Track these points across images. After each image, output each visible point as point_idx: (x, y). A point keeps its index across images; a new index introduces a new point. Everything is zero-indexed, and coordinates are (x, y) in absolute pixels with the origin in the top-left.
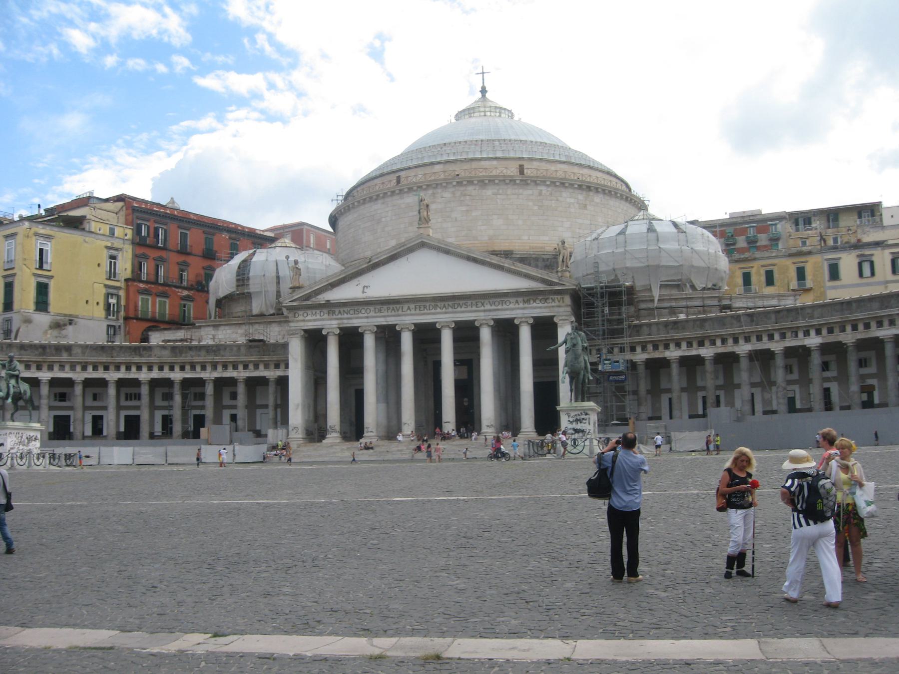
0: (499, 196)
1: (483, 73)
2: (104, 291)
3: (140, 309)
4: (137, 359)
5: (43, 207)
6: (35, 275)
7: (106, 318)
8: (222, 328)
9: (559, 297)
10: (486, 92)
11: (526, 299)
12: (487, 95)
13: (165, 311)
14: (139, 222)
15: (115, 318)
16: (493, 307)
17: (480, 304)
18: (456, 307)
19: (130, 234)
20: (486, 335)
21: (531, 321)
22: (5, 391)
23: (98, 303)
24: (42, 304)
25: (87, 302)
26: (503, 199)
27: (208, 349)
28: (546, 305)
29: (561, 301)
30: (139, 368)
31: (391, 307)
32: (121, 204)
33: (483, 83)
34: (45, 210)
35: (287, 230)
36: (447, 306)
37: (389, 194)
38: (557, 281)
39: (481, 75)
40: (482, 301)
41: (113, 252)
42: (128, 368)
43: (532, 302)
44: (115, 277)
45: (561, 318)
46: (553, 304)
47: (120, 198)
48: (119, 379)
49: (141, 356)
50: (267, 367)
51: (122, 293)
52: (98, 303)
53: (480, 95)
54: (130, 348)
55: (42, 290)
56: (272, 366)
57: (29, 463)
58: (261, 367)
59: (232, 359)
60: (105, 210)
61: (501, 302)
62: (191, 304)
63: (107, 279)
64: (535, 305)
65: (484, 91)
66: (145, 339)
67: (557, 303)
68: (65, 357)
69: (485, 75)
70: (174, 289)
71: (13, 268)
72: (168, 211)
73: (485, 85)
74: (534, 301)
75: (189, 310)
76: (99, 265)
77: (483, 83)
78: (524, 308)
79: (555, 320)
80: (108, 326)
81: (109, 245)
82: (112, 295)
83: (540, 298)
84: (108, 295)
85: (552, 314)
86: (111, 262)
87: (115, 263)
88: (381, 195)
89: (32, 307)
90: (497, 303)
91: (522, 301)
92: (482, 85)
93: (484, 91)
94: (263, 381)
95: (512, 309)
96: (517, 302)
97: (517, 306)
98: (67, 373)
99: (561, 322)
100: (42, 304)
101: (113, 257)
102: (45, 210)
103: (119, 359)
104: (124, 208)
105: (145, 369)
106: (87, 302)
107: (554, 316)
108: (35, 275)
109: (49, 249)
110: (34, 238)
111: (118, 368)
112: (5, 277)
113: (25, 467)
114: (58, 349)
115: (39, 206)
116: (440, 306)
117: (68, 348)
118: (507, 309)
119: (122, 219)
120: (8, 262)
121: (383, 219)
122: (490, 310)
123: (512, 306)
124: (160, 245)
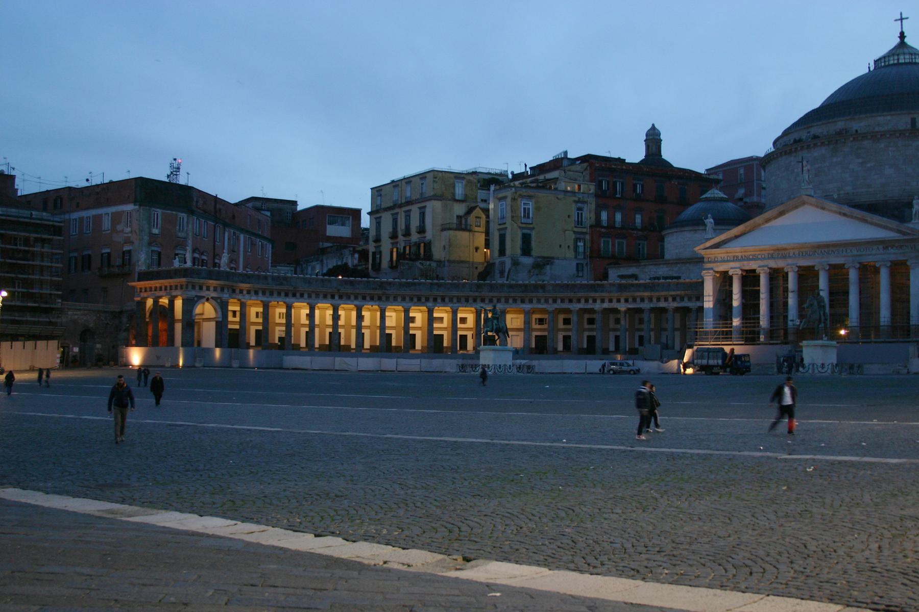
0: (890, 149)
1: (901, 19)
2: (573, 236)
3: (602, 249)
4: (592, 294)
5: (530, 165)
6: (520, 228)
7: (576, 257)
8: (662, 266)
10: (905, 37)
12: (906, 40)
13: (623, 250)
14: (600, 178)
15: (583, 257)
16: (859, 253)
17: (849, 251)
19: (592, 188)
20: (853, 275)
21: (889, 264)
22: (491, 327)
23: (569, 247)
24: (526, 250)
25: (560, 246)
26: (894, 151)
27: (646, 287)
30: (595, 301)
31: (781, 253)
32: (585, 165)
33: (902, 28)
34: (530, 168)
35: (740, 165)
37: (799, 148)
38: (910, 232)
39: (899, 22)
41: (579, 205)
42: (587, 301)
43: (890, 248)
44: (582, 225)
47: (588, 159)
48: (580, 309)
49: (596, 291)
50: (690, 299)
51: (588, 237)
52: (569, 247)
53: (898, 40)
54: (588, 285)
55: (526, 239)
56: (694, 299)
57: (505, 370)
58: (686, 299)
59: (663, 293)
60: (573, 171)
62: (646, 243)
63: (576, 227)
64: (892, 251)
65: (902, 36)
66: (605, 277)
68: (541, 294)
69: (903, 21)
70: (630, 231)
71: (505, 224)
72: (624, 167)
73: (904, 30)
74: (892, 248)
75: (643, 248)
76: (569, 216)
77: (902, 28)
79: (908, 263)
80: (577, 264)
81: (576, 199)
82: (580, 239)
84: (576, 240)
85: (904, 259)
86: (578, 213)
87: (582, 214)
88: (793, 150)
89: (519, 252)
90: (862, 250)
92: (900, 31)
93: (902, 36)
94: (686, 310)
95: (875, 255)
98: (543, 304)
100: (526, 250)
101: (580, 209)
102: (530, 168)
103: (579, 295)
104: (588, 168)
105: (599, 301)
106: (560, 246)
107: (907, 260)
108: (520, 228)
109: (530, 207)
110: (519, 199)
111: (579, 301)
112: (499, 230)
113: (502, 373)
114: (536, 287)
115: (526, 166)
117: (543, 287)
118: (869, 255)
119: (588, 177)
120: (501, 218)
121: (796, 170)
122: (857, 255)
123: (874, 252)
124: (618, 196)
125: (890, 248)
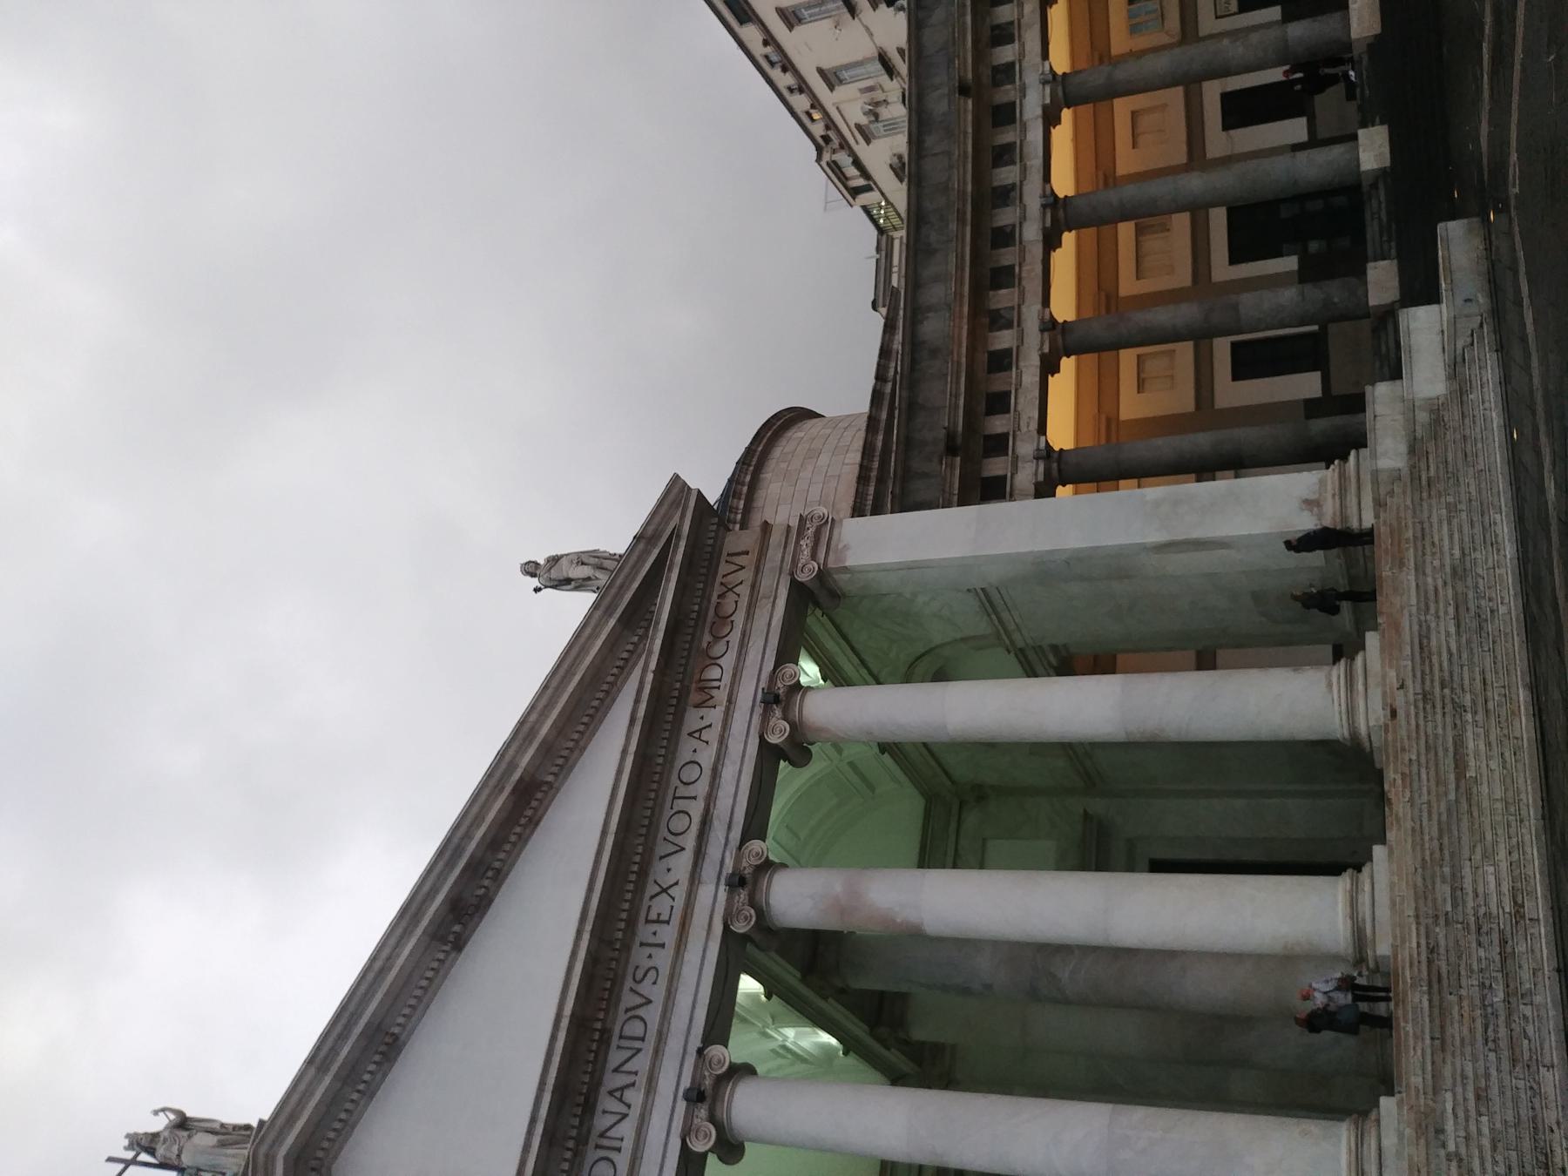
9: (724, 568)
11: (695, 697)
16: (690, 841)
18: (635, 1028)
28: (739, 618)
29: (741, 560)
36: (621, 1080)
40: (652, 889)
45: (807, 552)
46: (744, 590)
61: (680, 804)
64: (728, 662)
67: (746, 575)
78: (731, 701)
83: (707, 638)
91: (703, 712)
96: (697, 734)
97: (712, 735)
99: (821, 555)
116: (609, 1120)
125: (714, 673)
